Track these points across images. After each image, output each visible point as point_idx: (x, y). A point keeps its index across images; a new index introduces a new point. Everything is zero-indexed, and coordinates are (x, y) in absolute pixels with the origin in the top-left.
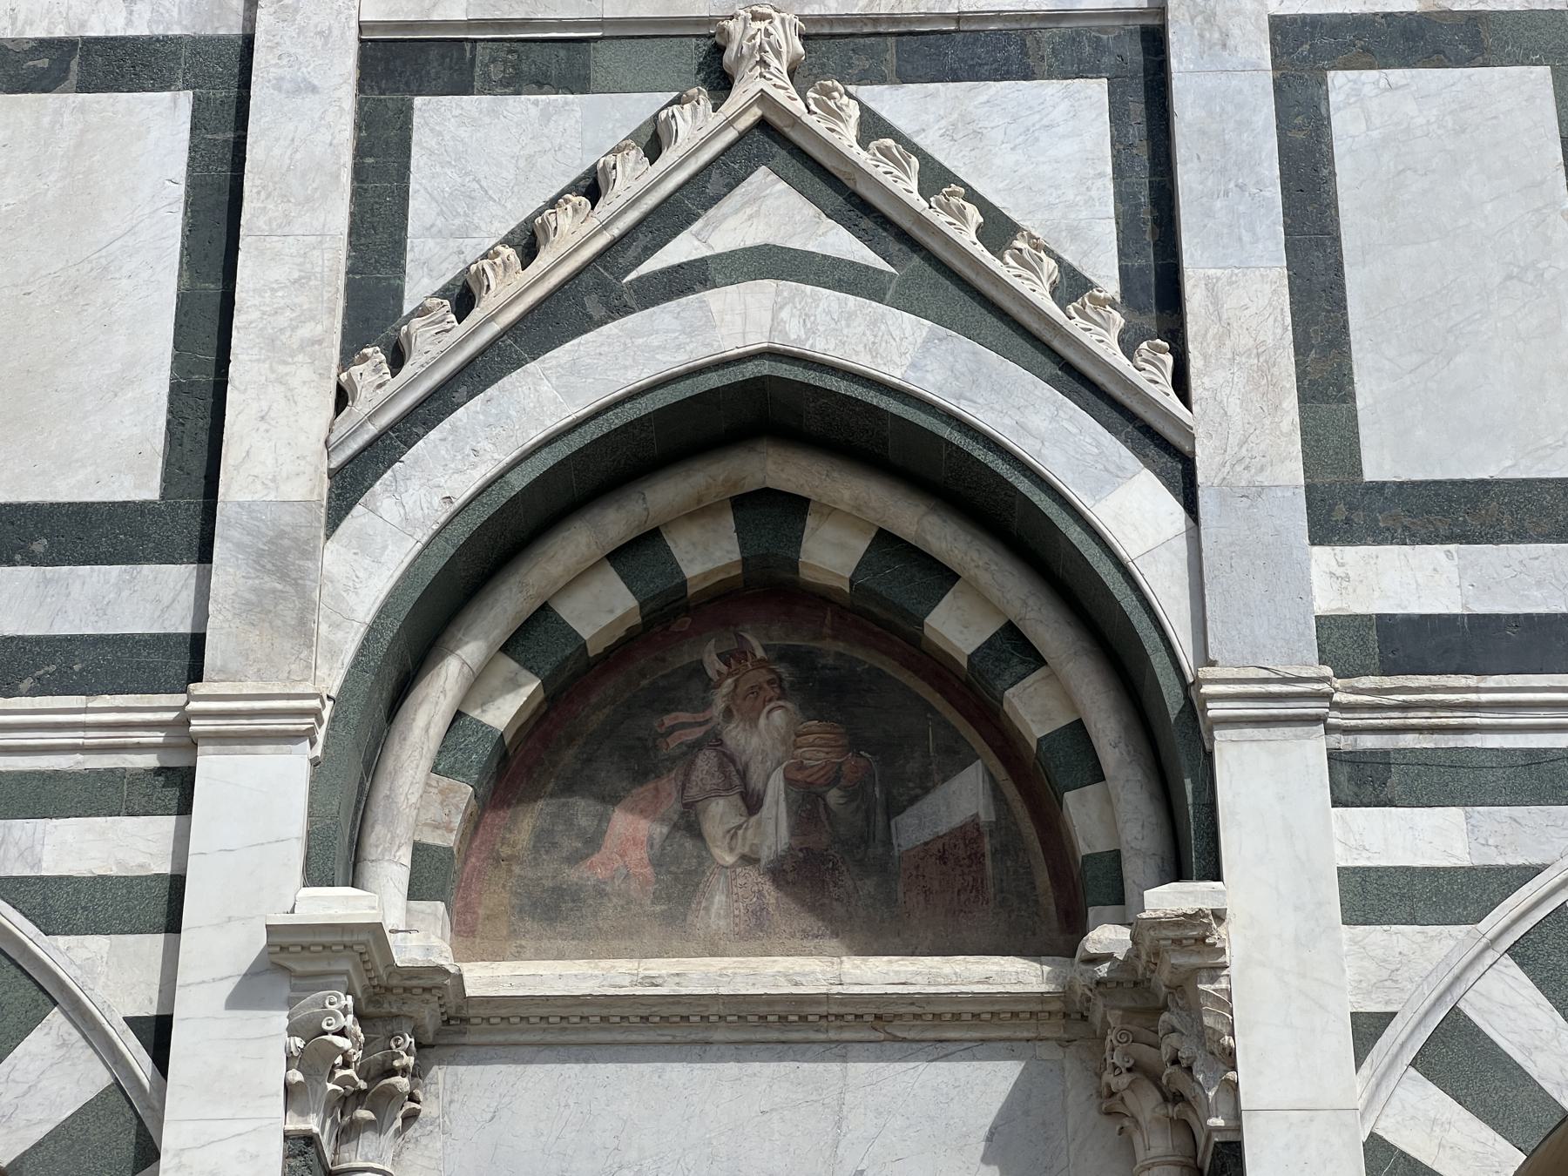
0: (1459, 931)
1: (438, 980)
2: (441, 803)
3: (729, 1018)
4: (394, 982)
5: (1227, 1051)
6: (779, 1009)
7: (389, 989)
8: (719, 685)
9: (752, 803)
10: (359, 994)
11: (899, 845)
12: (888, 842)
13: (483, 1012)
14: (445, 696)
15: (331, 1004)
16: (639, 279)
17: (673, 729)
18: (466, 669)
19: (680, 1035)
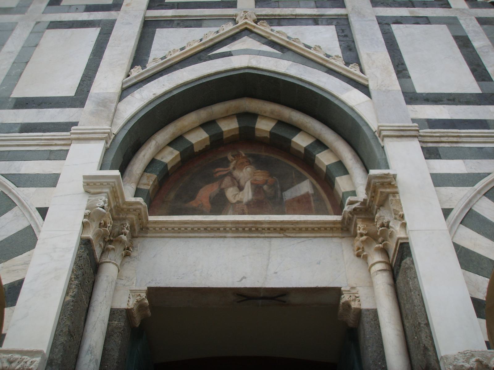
0: (469, 188)
1: (139, 206)
2: (147, 179)
3: (233, 229)
4: (125, 206)
5: (402, 216)
6: (249, 225)
7: (122, 209)
8: (232, 162)
9: (241, 188)
10: (113, 206)
11: (285, 199)
12: (282, 198)
13: (153, 225)
14: (150, 149)
15: (100, 200)
16: (213, 54)
17: (218, 172)
18: (157, 144)
19: (217, 234)
